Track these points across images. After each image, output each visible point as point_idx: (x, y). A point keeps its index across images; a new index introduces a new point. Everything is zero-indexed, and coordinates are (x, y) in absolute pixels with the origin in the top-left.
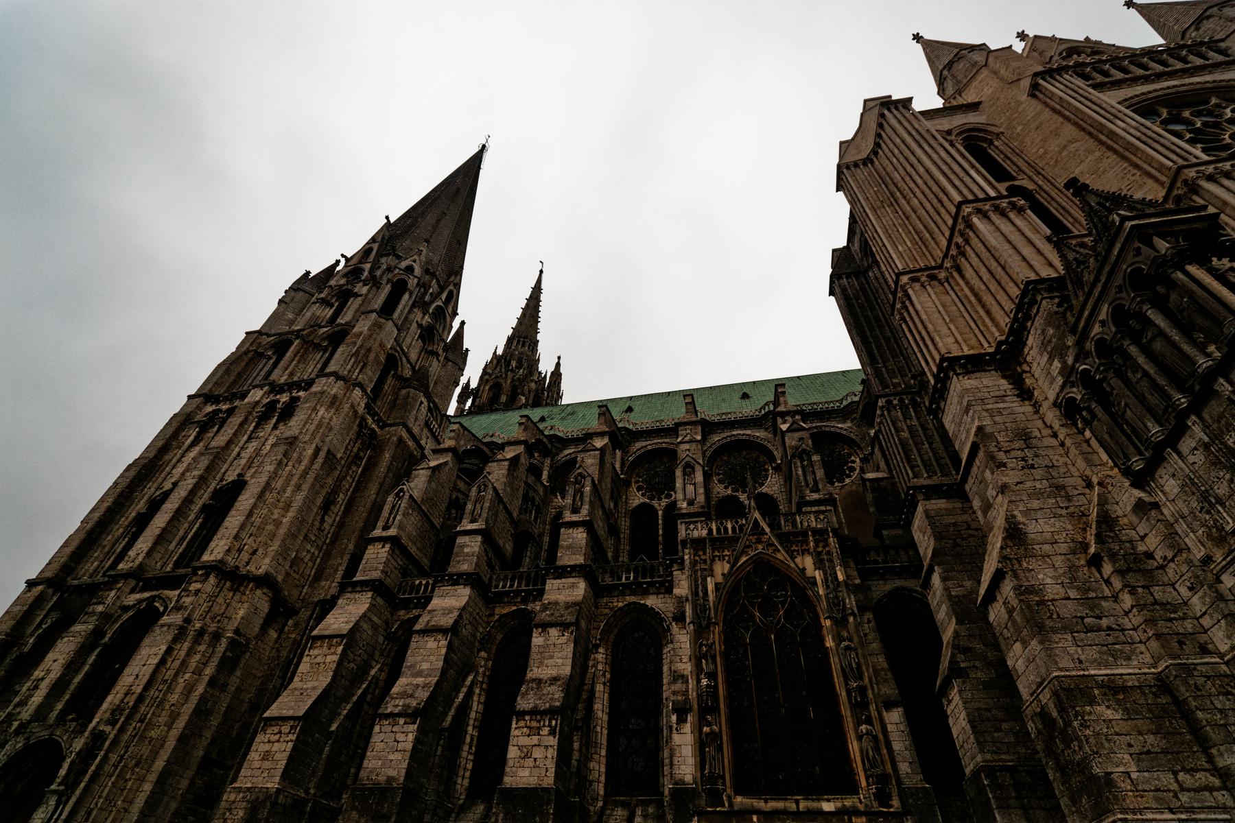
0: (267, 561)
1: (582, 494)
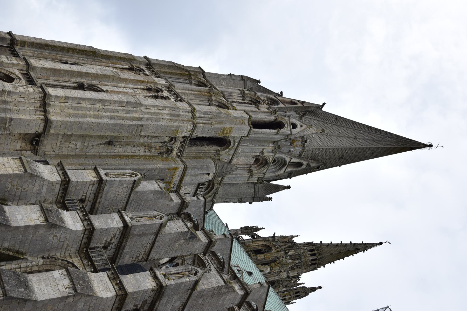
0: (59, 119)
1: (182, 277)
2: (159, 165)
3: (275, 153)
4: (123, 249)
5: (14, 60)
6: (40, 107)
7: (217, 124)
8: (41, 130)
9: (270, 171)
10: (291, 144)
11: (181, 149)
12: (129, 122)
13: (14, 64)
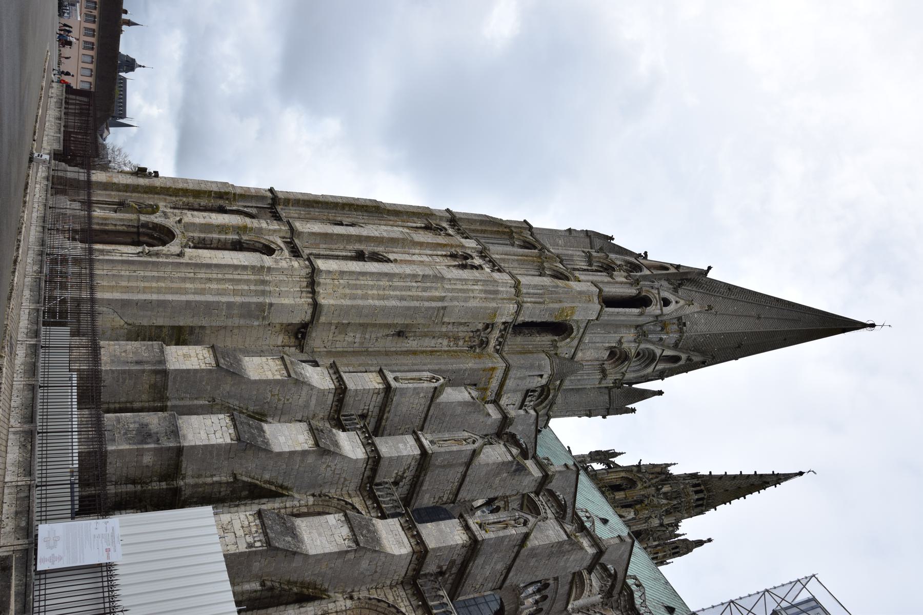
0: (332, 302)
2: (470, 364)
3: (639, 343)
4: (421, 485)
5: (275, 226)
6: (307, 287)
8: (308, 318)
9: (633, 369)
10: (662, 329)
11: (501, 340)
12: (427, 304)
13: (275, 231)
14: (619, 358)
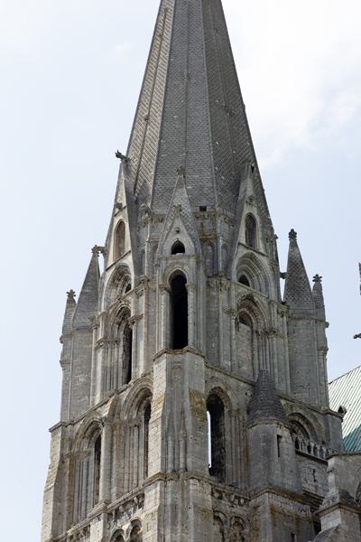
7: (184, 425)
14: (249, 308)
